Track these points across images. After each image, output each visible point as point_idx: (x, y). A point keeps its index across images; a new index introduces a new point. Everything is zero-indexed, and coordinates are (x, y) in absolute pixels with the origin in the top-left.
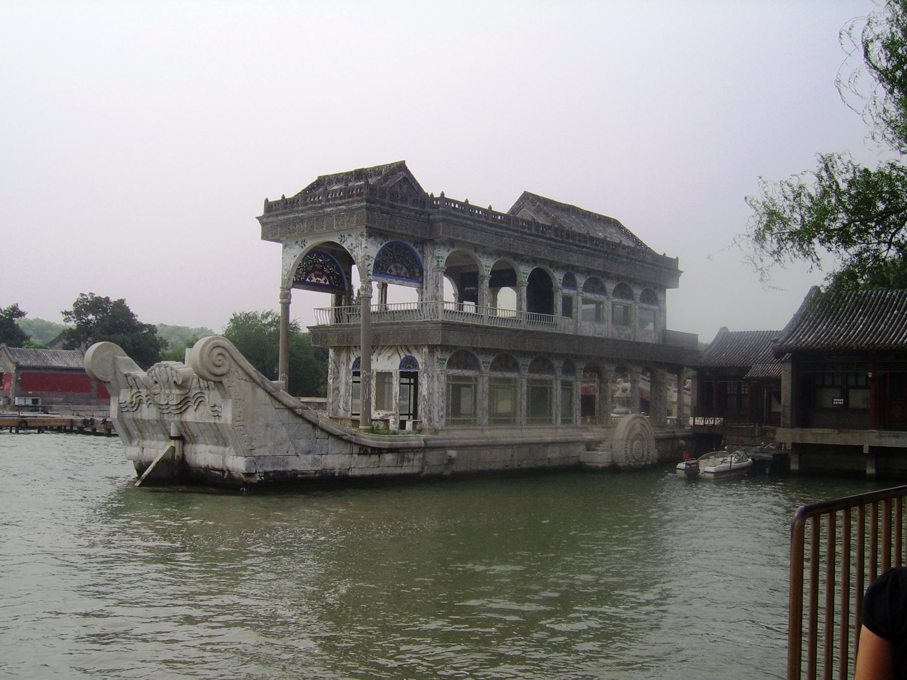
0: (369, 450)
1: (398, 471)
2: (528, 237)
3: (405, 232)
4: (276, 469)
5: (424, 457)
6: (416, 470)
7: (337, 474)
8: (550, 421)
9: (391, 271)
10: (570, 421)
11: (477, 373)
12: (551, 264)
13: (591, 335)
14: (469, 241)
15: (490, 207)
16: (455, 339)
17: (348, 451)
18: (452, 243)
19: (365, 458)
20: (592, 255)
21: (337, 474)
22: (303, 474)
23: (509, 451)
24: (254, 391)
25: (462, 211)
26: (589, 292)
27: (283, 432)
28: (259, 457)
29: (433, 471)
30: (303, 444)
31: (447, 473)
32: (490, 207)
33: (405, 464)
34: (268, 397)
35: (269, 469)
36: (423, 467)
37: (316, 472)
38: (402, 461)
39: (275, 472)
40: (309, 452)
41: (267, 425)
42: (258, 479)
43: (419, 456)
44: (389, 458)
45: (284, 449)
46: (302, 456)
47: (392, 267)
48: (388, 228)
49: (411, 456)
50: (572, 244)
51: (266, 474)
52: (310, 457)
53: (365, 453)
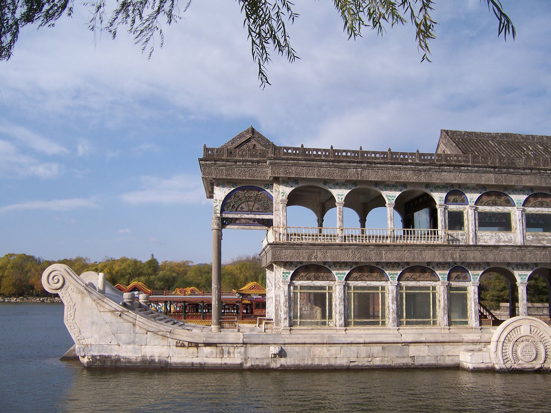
0: (186, 344)
1: (218, 361)
2: (378, 165)
3: (244, 178)
4: (102, 354)
5: (246, 353)
6: (238, 361)
7: (157, 360)
8: (434, 323)
9: (242, 208)
10: (466, 323)
11: (332, 283)
12: (428, 185)
13: (492, 243)
14: (305, 177)
15: (332, 147)
16: (287, 255)
17: (166, 344)
18: (295, 181)
19: (183, 350)
20: (476, 172)
21: (157, 360)
22: (126, 359)
23: (354, 348)
24: (83, 299)
25: (295, 154)
26: (489, 205)
27: (107, 328)
28: (87, 345)
29: (258, 363)
30: (124, 337)
31: (275, 364)
32: (332, 147)
33: (226, 356)
34: (94, 304)
35: (95, 354)
36: (246, 359)
37: (137, 357)
38: (222, 352)
39: (100, 356)
40: (129, 344)
41: (93, 323)
42: (88, 360)
43: (243, 349)
44: (208, 349)
45: (108, 340)
46: (124, 346)
47: (243, 205)
48: (224, 177)
49: (232, 350)
50: (443, 165)
51: (93, 357)
52: (130, 347)
53: (183, 346)
